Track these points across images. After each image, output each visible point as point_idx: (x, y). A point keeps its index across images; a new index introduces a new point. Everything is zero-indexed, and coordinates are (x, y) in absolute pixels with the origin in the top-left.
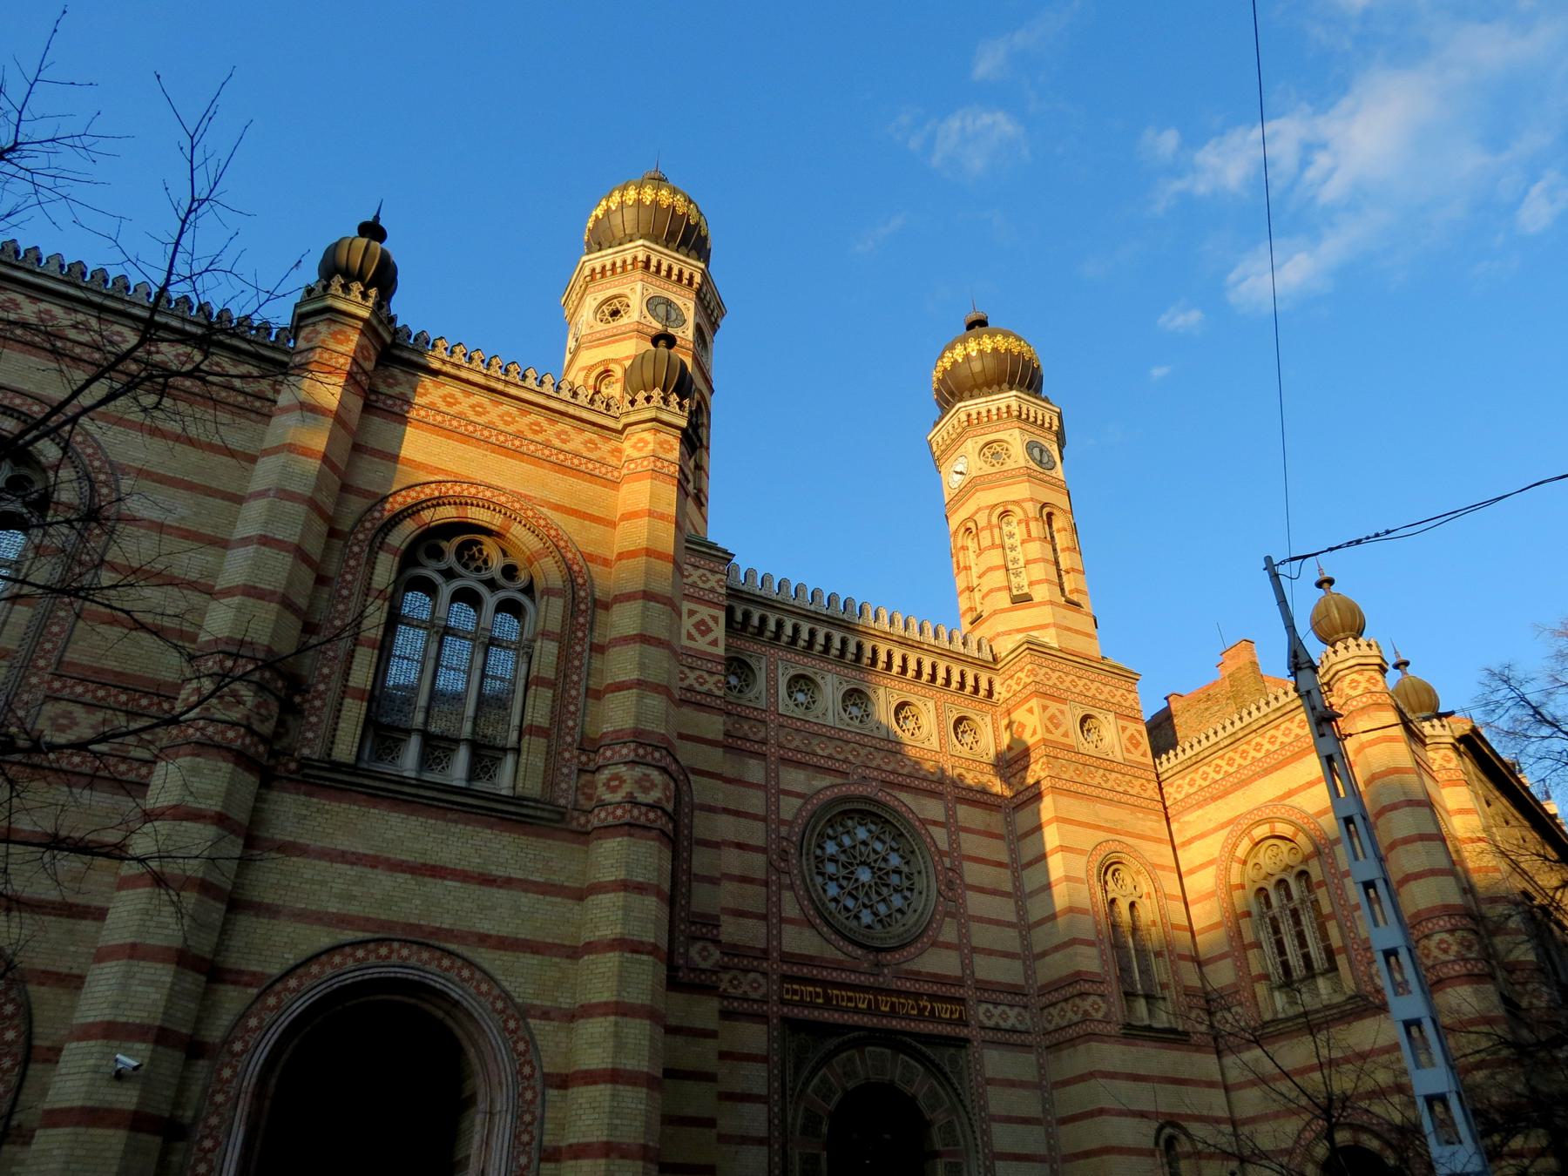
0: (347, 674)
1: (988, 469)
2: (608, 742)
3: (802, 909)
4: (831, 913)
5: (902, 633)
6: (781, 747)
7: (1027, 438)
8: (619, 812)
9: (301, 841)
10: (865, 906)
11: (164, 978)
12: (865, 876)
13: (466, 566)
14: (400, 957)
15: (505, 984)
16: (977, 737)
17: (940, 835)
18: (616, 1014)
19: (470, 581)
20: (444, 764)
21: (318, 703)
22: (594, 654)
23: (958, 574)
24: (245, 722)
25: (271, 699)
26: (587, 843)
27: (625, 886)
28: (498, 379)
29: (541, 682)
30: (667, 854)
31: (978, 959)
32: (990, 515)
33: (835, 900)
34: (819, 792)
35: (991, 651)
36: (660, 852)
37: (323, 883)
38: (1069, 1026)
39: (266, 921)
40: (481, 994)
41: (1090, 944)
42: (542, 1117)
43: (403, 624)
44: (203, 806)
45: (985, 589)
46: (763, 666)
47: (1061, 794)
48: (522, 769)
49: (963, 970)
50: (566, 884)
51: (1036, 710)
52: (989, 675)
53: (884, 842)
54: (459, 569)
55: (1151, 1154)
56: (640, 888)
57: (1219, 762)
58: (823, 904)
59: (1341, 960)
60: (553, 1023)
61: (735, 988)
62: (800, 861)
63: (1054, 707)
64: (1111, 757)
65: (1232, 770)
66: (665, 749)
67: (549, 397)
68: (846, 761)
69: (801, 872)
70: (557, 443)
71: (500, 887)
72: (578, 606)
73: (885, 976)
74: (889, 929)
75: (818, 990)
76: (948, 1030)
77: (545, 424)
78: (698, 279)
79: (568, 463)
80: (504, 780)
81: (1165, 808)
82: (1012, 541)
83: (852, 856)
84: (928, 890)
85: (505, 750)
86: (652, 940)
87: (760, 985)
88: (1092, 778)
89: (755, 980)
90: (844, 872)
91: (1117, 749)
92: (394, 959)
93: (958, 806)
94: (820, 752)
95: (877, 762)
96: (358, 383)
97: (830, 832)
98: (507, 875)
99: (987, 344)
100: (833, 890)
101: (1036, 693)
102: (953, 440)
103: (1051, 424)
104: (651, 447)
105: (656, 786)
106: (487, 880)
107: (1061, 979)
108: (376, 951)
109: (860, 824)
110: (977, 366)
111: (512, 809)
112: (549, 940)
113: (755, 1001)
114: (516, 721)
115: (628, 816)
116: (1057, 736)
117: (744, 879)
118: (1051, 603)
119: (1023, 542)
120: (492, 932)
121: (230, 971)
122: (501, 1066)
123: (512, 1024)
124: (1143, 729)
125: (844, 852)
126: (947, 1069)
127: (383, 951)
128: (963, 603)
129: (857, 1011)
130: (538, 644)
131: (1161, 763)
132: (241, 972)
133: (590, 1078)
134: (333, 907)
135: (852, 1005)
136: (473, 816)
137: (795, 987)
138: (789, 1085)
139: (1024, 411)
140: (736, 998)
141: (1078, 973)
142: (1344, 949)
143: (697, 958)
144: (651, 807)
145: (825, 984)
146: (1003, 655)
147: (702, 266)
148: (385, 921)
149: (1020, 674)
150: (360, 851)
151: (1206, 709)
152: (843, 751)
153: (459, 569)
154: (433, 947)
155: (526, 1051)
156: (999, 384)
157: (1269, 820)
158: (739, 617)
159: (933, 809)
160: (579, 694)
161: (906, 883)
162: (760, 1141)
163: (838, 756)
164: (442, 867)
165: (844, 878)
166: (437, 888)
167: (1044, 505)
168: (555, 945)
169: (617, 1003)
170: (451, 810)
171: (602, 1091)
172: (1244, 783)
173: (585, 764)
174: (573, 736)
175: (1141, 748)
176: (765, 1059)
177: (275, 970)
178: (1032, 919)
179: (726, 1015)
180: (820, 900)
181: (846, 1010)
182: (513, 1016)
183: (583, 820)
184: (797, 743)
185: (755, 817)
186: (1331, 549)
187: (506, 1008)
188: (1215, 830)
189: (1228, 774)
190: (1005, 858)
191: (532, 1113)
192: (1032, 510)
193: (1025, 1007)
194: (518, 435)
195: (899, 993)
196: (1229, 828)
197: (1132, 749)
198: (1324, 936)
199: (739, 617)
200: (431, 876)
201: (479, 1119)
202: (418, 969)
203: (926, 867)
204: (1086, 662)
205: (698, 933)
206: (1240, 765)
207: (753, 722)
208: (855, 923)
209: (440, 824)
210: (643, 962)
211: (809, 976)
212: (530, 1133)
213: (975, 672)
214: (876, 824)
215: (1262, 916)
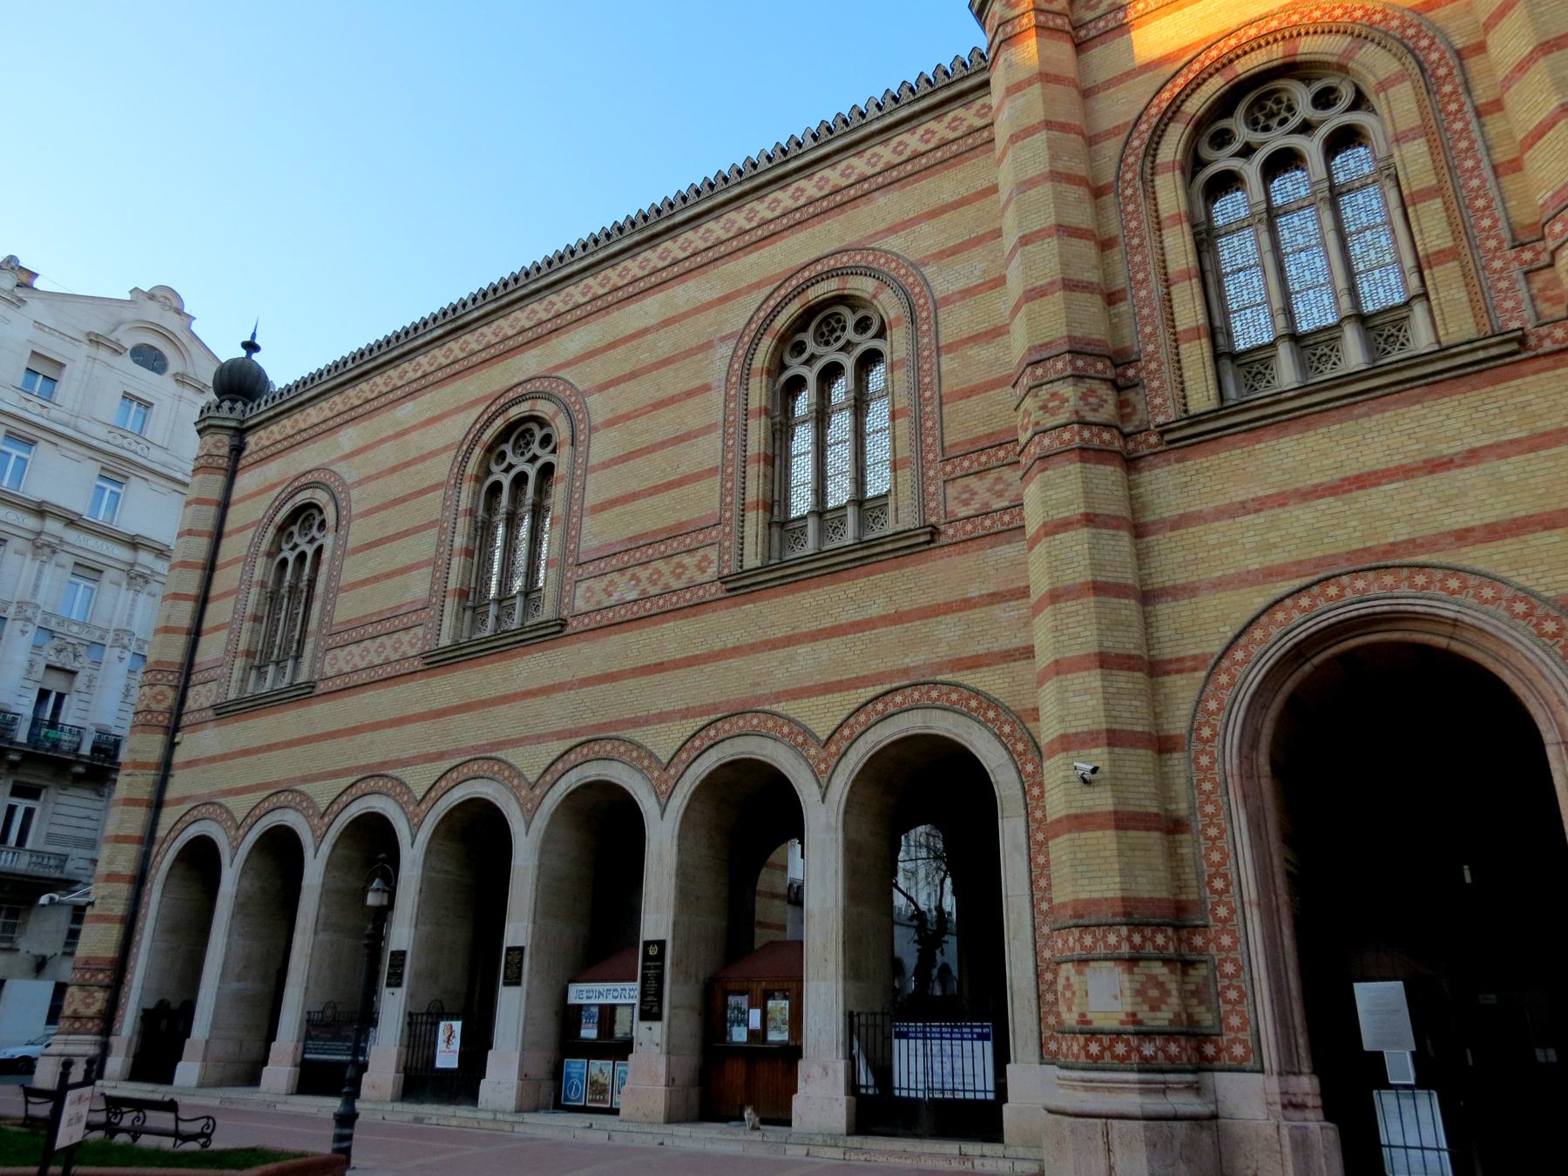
0: (1171, 320)
9: (1192, 509)
11: (1093, 685)
13: (1266, 129)
14: (1355, 591)
19: (1277, 140)
20: (1334, 359)
21: (1153, 366)
22: (1486, 119)
24: (1074, 418)
25: (1096, 385)
37: (1232, 543)
39: (1186, 601)
43: (1220, 236)
44: (1067, 514)
48: (1437, 313)
54: (1256, 137)
71: (1462, 466)
80: (1421, 338)
92: (1349, 595)
96: (1055, 30)
98: (1467, 447)
108: (1323, 593)
120: (1472, 524)
121: (1170, 661)
127: (1332, 591)
132: (1181, 660)
134: (1254, 563)
148: (1320, 558)
150: (1261, 494)
164: (1369, 474)
166: (1373, 498)
174: (1497, 236)
177: (1217, 647)
182: (1547, 617)
200: (1359, 488)
202: (1384, 598)
209: (1349, 426)
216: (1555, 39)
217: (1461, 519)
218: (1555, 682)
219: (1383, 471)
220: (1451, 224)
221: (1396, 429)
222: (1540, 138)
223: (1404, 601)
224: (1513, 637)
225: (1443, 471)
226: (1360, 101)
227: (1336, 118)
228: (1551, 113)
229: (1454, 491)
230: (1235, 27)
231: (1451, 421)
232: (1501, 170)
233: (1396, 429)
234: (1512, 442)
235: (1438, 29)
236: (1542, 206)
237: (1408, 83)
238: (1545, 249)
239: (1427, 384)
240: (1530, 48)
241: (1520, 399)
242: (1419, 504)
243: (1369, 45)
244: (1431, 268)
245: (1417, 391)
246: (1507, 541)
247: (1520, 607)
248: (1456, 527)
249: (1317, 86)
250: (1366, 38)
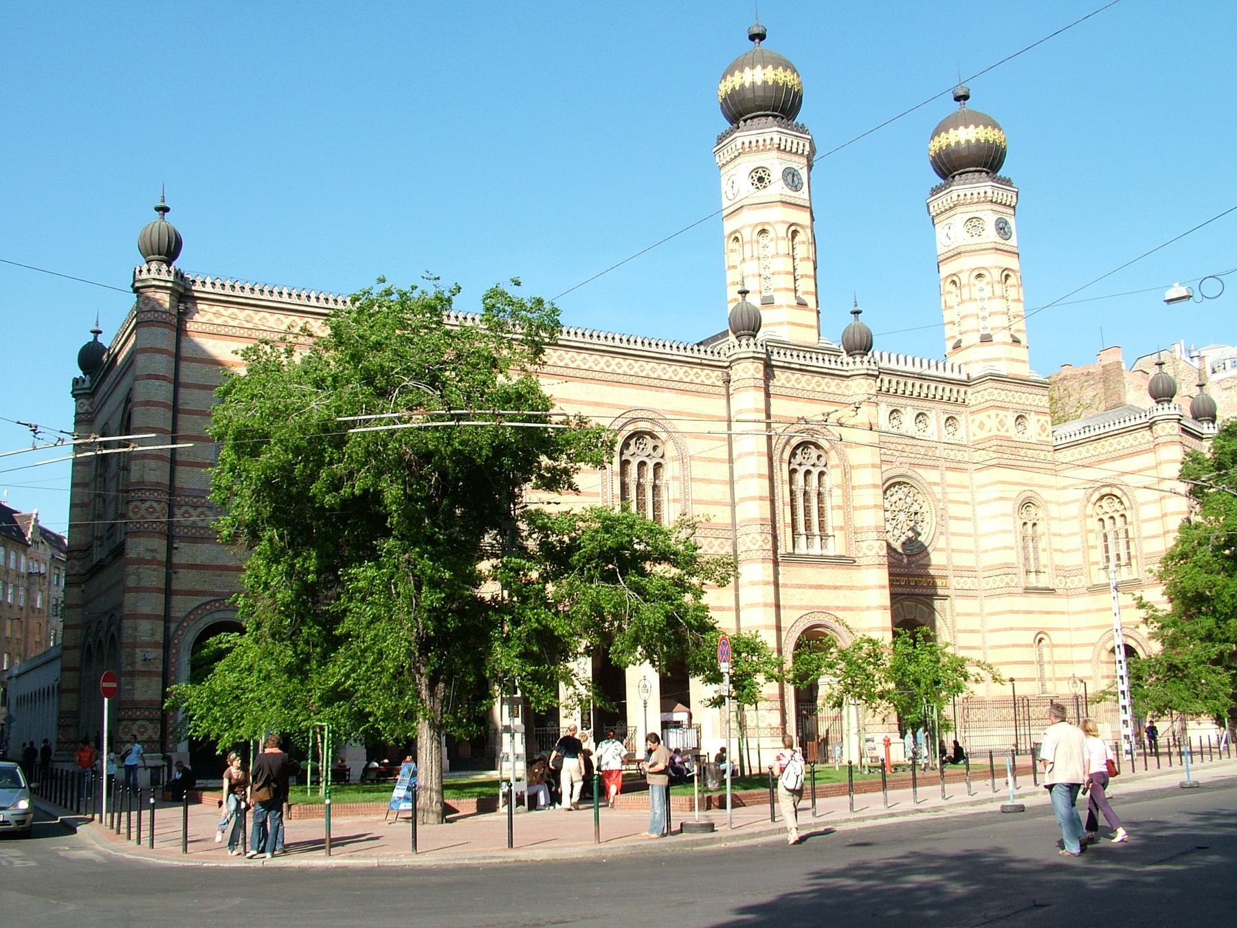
7: (996, 217)
17: (937, 489)
31: (954, 555)
41: (1012, 548)
59: (1133, 561)
63: (1002, 413)
65: (1095, 453)
70: (827, 390)
78: (807, 148)
106: (836, 588)
116: (1003, 433)
124: (1048, 418)
134: (798, 603)
159: (931, 476)
161: (920, 519)
198: (1128, 548)
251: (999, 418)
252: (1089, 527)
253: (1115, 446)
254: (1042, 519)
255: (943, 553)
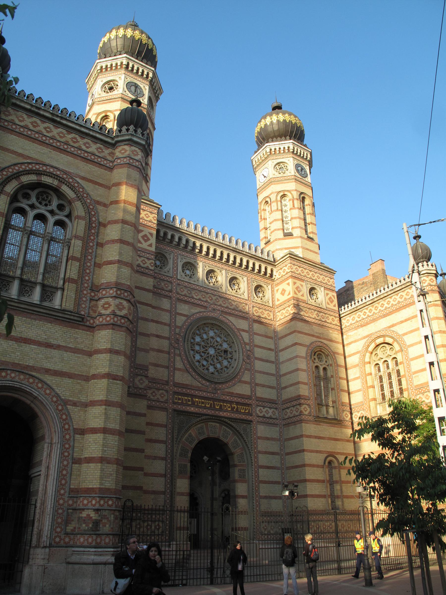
1: (277, 175)
2: (104, 287)
3: (184, 364)
4: (196, 367)
5: (235, 246)
6: (178, 294)
7: (296, 162)
8: (108, 319)
10: (211, 364)
12: (212, 351)
13: (40, 203)
14: (11, 377)
15: (57, 390)
16: (264, 294)
17: (245, 336)
18: (105, 405)
19: (42, 210)
20: (30, 293)
22: (98, 247)
23: (261, 221)
26: (93, 332)
27: (111, 351)
28: (57, 116)
29: (74, 258)
30: (129, 338)
31: (258, 389)
32: (277, 196)
33: (199, 361)
34: (193, 315)
35: (273, 256)
36: (126, 337)
38: (294, 417)
40: (46, 394)
42: (74, 446)
43: (11, 228)
45: (272, 229)
46: (172, 257)
47: (299, 321)
49: (251, 393)
50: (84, 349)
51: (291, 284)
52: (271, 267)
53: (221, 338)
54: (37, 204)
55: (322, 467)
56: (117, 352)
57: (365, 311)
58: (194, 363)
60: (78, 408)
61: (154, 396)
62: (184, 344)
63: (299, 283)
64: (320, 306)
65: (370, 314)
66: (129, 291)
67: (81, 126)
68: (206, 301)
69: (184, 348)
70: (84, 148)
71: (55, 349)
72: (91, 224)
73: (218, 394)
74: (221, 375)
75: (189, 398)
76: (244, 417)
77: (79, 139)
78: (151, 75)
79: (89, 158)
80: (57, 302)
81: (341, 329)
82: (286, 208)
83: (206, 344)
84: (239, 359)
85: (57, 288)
86: (122, 375)
87: (165, 396)
88: (312, 315)
89: (162, 394)
90: (203, 350)
91: (324, 303)
93: (254, 324)
94: (195, 297)
95: (220, 302)
97: (198, 332)
98: (58, 344)
99: (281, 117)
100: (198, 357)
101: (292, 277)
102: (263, 160)
103: (307, 157)
104: (128, 153)
105: (125, 308)
106: (49, 346)
107: (292, 398)
109: (211, 330)
110: (276, 128)
111: (60, 315)
112: (77, 373)
113: (162, 402)
114: (62, 276)
115: (112, 321)
117: (159, 351)
118: (301, 237)
119: (291, 209)
120: (51, 368)
122: (56, 425)
123: (60, 408)
124: (335, 295)
125: (203, 341)
126: (242, 432)
128: (262, 235)
129: (205, 407)
130: (73, 241)
131: (341, 310)
133: (94, 431)
135: (204, 405)
136: (43, 317)
137: (180, 397)
138: (175, 437)
139: (296, 150)
140: (154, 401)
141: (299, 396)
142: (407, 389)
143: (138, 383)
144: (122, 317)
145: (193, 396)
146: (278, 259)
147: (153, 69)
149: (285, 268)
151: (362, 288)
152: (205, 297)
153: (37, 204)
154: (25, 373)
155: (66, 419)
156: (285, 137)
157: (383, 336)
158: (162, 234)
160: (91, 265)
162: (162, 459)
163: (203, 299)
164: (29, 339)
165: (203, 352)
166: (27, 348)
167: (302, 193)
168: (79, 375)
169: (106, 400)
170: (33, 314)
171: (99, 437)
172: (374, 320)
173: (93, 297)
175: (334, 303)
176: (165, 426)
178: (282, 373)
179: (149, 407)
180: (192, 361)
181: (201, 407)
182: (60, 404)
183: (92, 321)
184: (185, 292)
185: (165, 324)
186: (431, 222)
187: (58, 400)
188: (361, 339)
189: (369, 316)
190: (273, 347)
191: (69, 444)
192: (296, 195)
193: (276, 409)
194: (66, 143)
195: (224, 401)
196: (367, 339)
197: (330, 303)
199: (162, 234)
200: (24, 343)
201: (46, 446)
202: (19, 383)
203: (239, 349)
204: (314, 264)
205: (139, 373)
206: (374, 313)
207: (166, 282)
208: (207, 371)
210: (118, 384)
211: (186, 392)
212: (68, 452)
213: (265, 265)
214: (218, 330)
215: (376, 375)
216: (124, 241)
217: (49, 366)
218: (56, 425)
219: (33, 340)
220: (79, 273)
221: (41, 328)
222: (110, 264)
223: (24, 386)
224: (50, 408)
225: (49, 348)
226: (69, 216)
227: (61, 216)
228: (115, 260)
229: (50, 356)
230: (47, 164)
231: (57, 334)
232: (96, 265)
233: (41, 328)
234: (70, 348)
235: (97, 212)
236: (102, 283)
237: (84, 222)
238: (97, 295)
239: (55, 319)
240: (117, 238)
241: (77, 336)
242: (39, 356)
243: (79, 202)
244: (69, 282)
245: (51, 319)
246: (58, 377)
247: (55, 399)
248: (47, 367)
249: (61, 202)
250: (80, 199)
251: (296, 286)
252: (368, 371)
253: (386, 305)
254: (331, 365)
255: (248, 386)
